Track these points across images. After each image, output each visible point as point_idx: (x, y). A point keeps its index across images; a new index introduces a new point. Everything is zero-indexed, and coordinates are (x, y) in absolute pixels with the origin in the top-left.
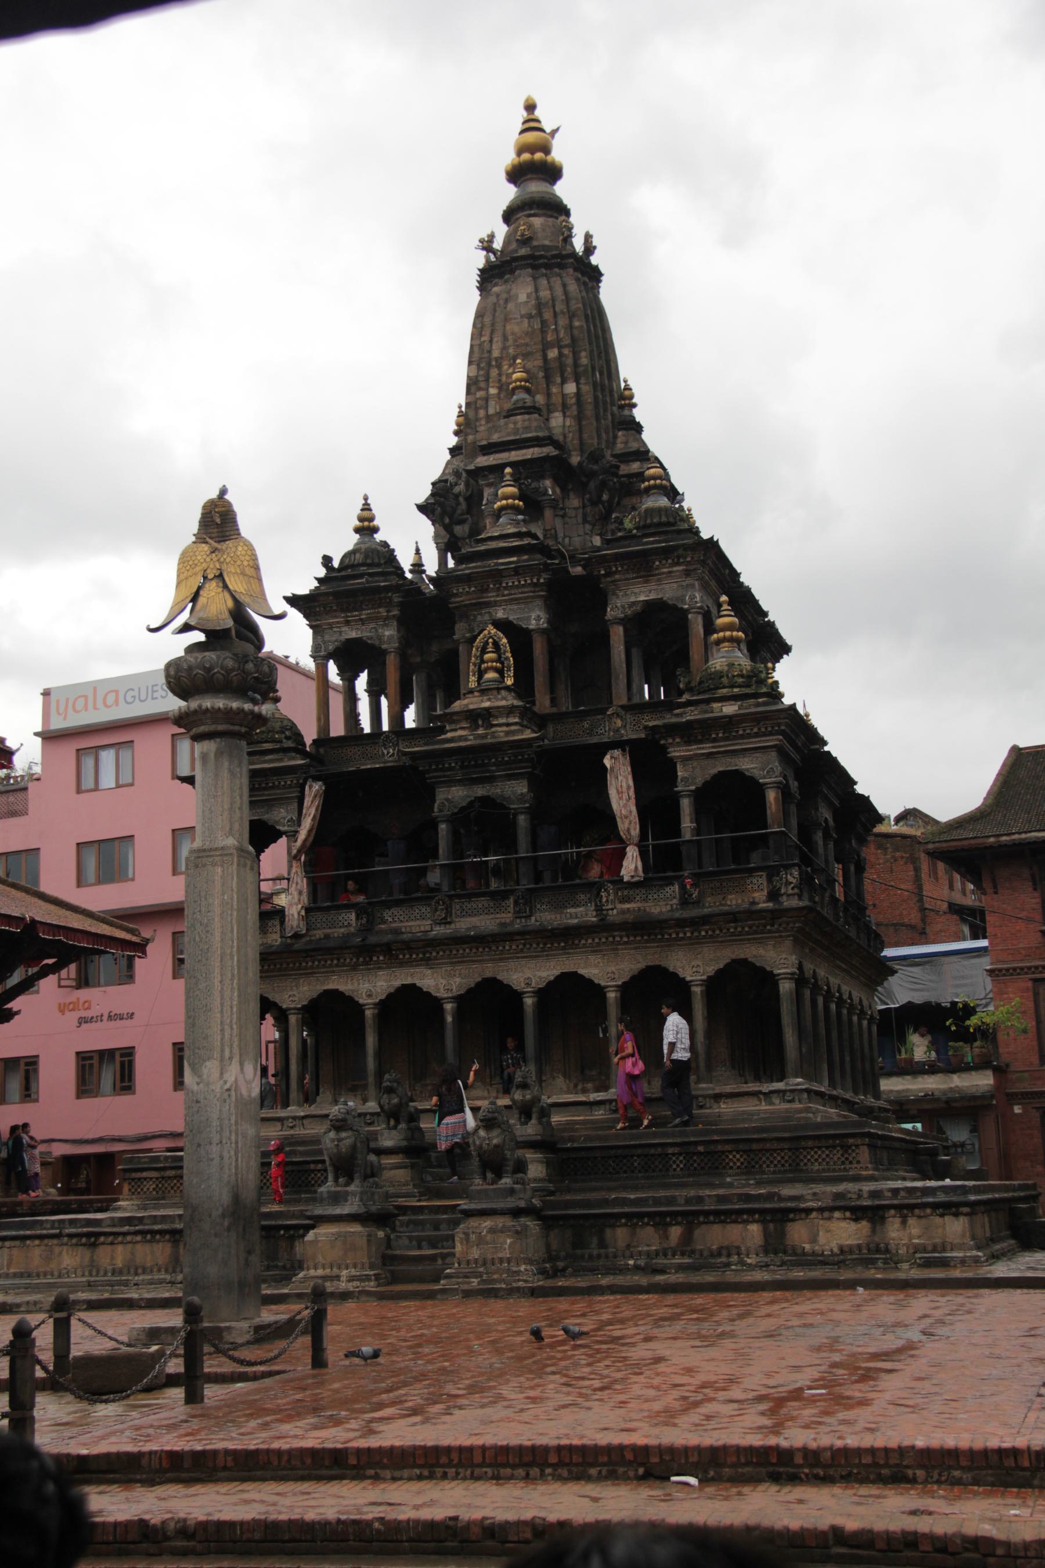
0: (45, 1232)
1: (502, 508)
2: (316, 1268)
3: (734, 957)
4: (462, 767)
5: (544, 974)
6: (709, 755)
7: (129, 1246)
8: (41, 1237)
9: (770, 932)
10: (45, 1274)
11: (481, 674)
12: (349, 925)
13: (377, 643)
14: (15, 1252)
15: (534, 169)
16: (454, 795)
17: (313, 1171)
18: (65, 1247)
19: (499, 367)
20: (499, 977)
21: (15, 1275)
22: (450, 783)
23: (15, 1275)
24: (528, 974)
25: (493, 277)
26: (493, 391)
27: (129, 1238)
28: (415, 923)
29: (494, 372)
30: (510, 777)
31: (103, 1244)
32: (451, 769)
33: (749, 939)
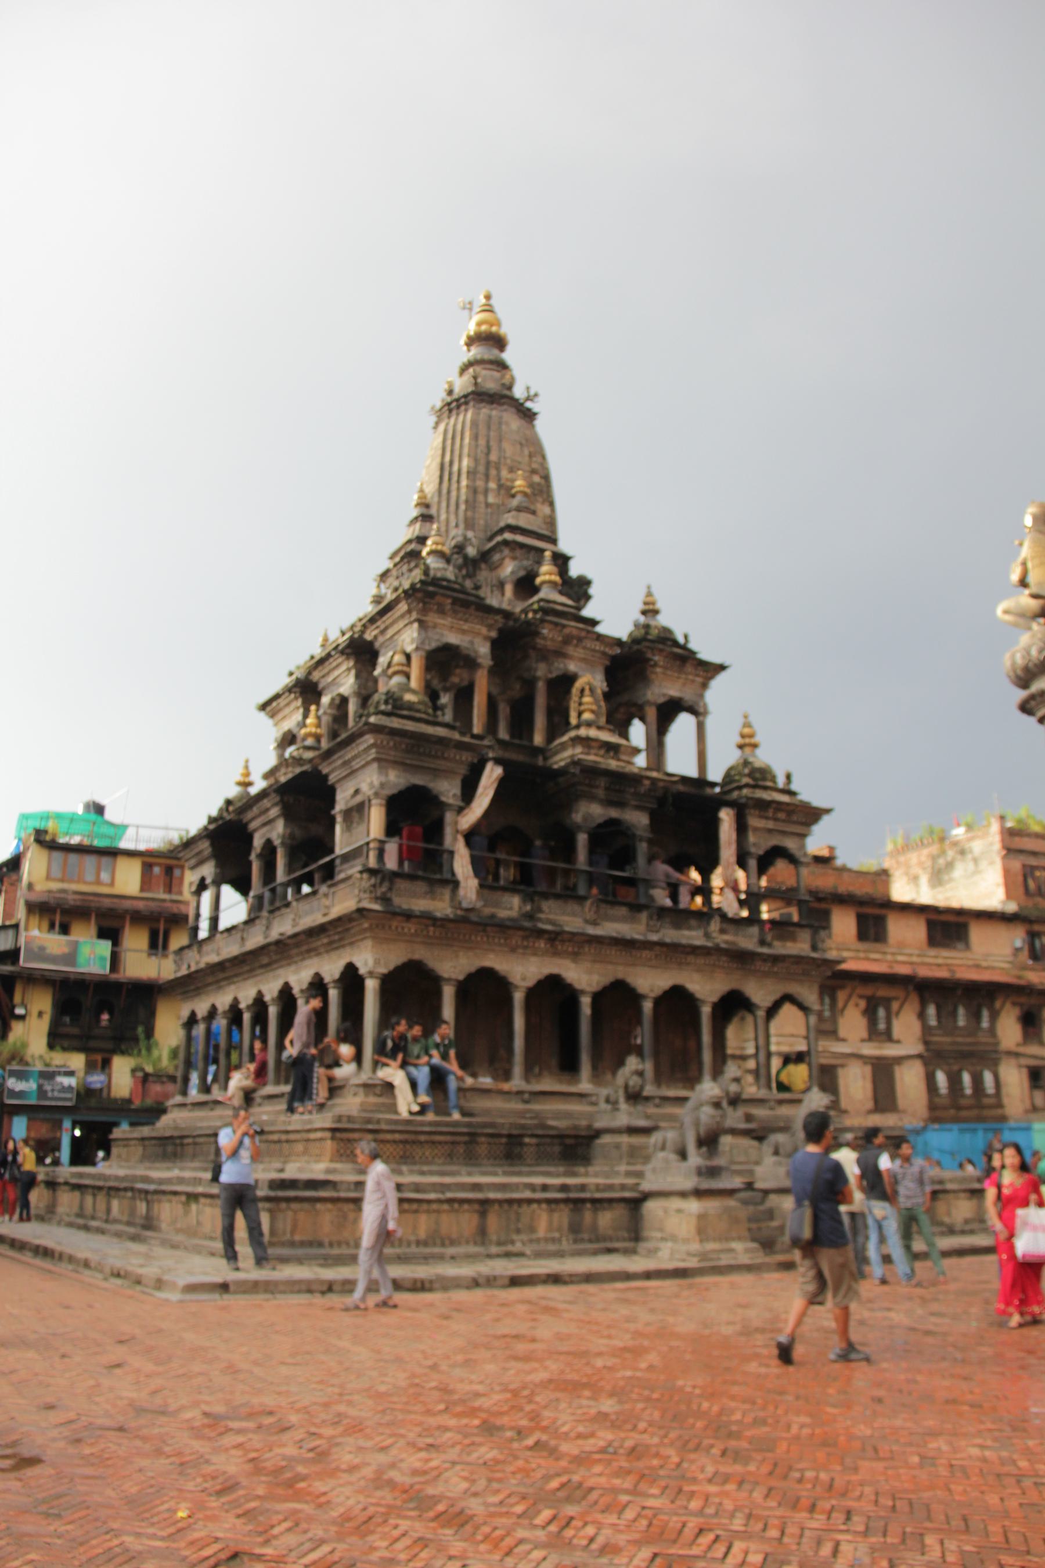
0: (343, 1194)
6: (770, 831)
7: (434, 1216)
10: (339, 1244)
11: (580, 714)
12: (511, 909)
13: (473, 654)
14: (301, 1216)
16: (590, 812)
19: (498, 469)
21: (303, 1244)
22: (592, 798)
23: (303, 1244)
24: (651, 981)
26: (492, 485)
27: (434, 1206)
28: (571, 919)
29: (493, 472)
30: (638, 808)
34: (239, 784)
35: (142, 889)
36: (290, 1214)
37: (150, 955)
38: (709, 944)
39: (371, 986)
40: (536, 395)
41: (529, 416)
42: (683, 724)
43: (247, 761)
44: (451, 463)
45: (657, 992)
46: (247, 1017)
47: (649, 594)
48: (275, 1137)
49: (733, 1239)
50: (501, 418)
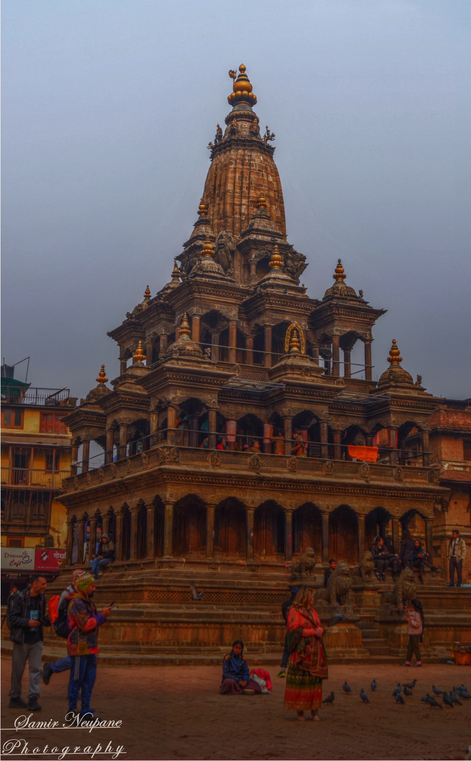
1: (277, 264)
2: (338, 647)
3: (412, 508)
4: (302, 394)
5: (334, 504)
8: (144, 622)
9: (428, 498)
11: (290, 348)
15: (242, 97)
17: (250, 594)
18: (158, 629)
20: (314, 502)
21: (128, 643)
25: (238, 145)
26: (244, 201)
31: (181, 628)
32: (296, 393)
33: (418, 501)
34: (98, 380)
35: (41, 431)
36: (122, 628)
37: (46, 473)
38: (363, 482)
39: (169, 508)
40: (273, 135)
41: (269, 151)
42: (359, 346)
43: (103, 367)
44: (220, 186)
45: (331, 510)
46: (105, 520)
47: (339, 265)
48: (118, 590)
49: (353, 647)
50: (251, 156)
